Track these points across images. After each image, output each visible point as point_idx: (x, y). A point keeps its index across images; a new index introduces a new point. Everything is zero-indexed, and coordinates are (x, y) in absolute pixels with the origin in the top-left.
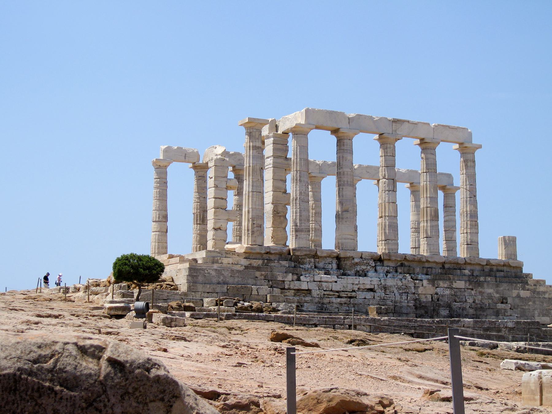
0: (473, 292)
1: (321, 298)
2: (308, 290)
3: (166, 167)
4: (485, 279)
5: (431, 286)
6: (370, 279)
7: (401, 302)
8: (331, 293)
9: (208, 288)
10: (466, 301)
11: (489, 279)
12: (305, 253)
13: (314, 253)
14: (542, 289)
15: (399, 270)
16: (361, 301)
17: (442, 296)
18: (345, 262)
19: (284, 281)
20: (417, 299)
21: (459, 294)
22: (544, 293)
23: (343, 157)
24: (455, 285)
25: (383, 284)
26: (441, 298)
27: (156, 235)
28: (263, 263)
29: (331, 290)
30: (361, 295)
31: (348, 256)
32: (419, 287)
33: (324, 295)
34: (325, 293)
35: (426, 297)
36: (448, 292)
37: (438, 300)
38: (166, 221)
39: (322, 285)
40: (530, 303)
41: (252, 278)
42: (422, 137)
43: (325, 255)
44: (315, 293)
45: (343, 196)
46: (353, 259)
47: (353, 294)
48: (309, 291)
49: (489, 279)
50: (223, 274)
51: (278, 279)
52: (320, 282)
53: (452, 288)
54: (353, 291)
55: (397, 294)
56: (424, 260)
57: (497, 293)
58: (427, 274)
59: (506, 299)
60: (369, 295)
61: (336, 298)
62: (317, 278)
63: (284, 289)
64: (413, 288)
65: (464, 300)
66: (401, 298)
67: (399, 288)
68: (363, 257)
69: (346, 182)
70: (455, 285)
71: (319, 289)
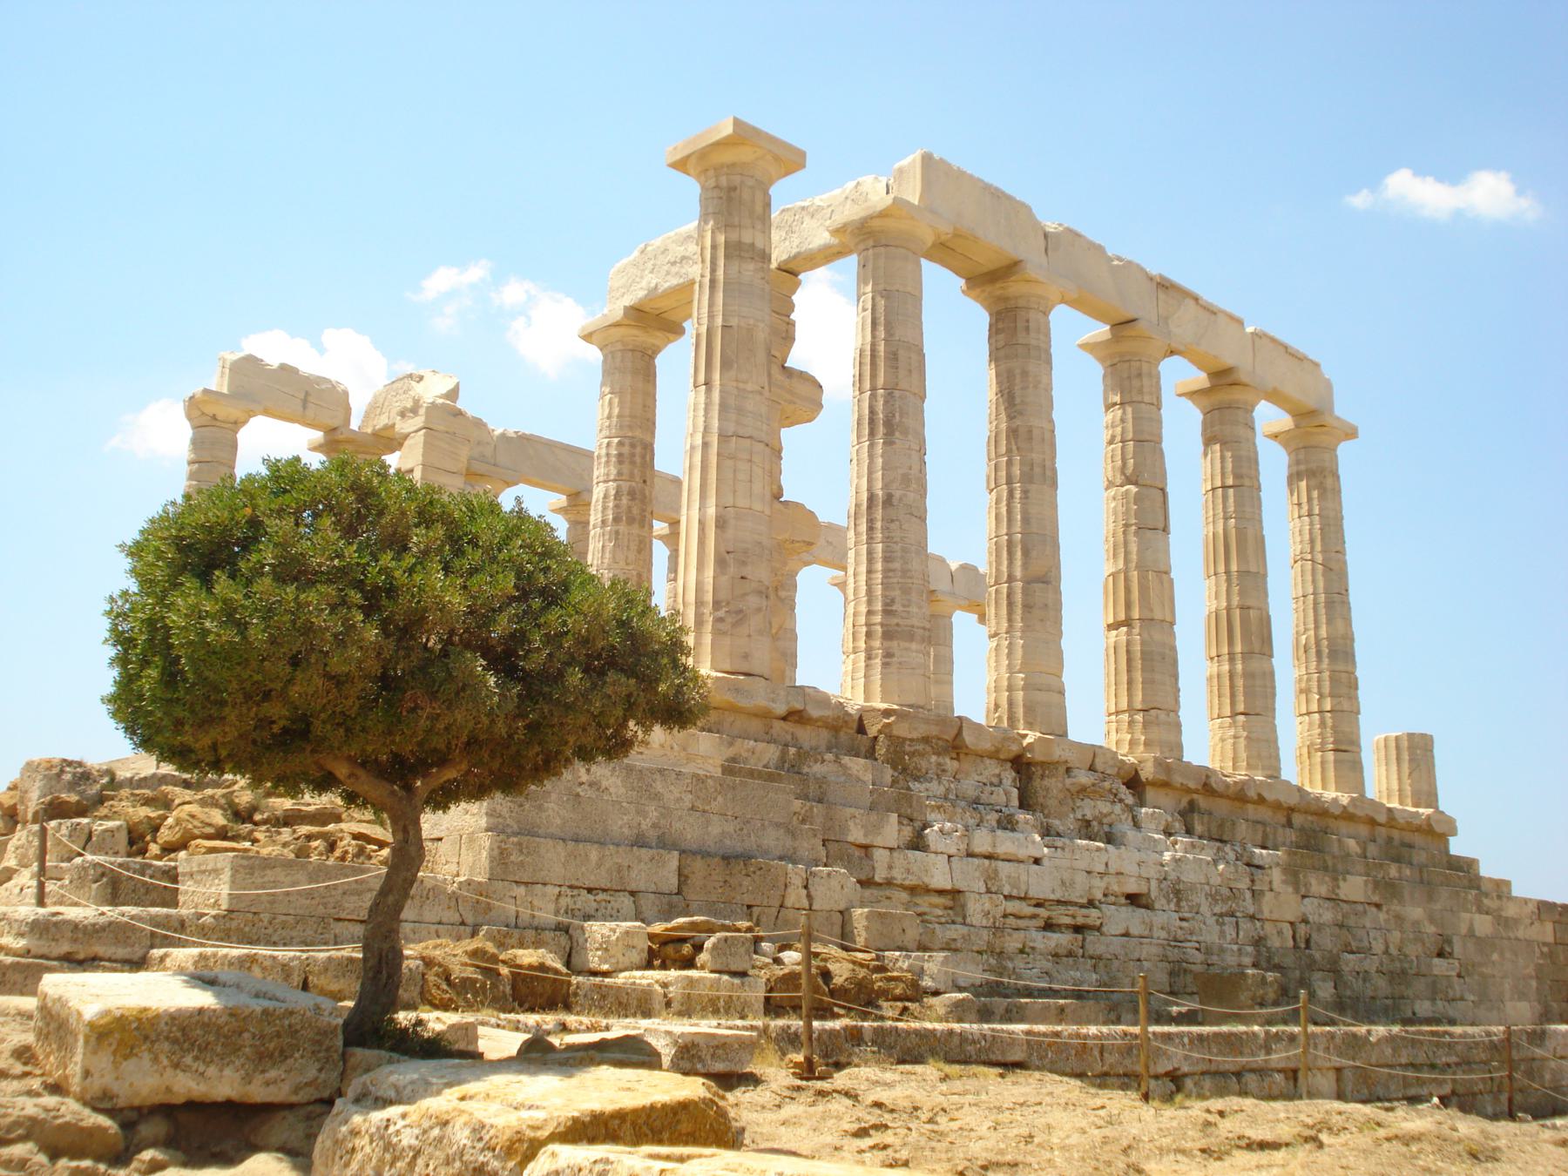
0: (1382, 916)
1: (997, 929)
2: (955, 893)
3: (237, 424)
5: (1290, 889)
6: (1137, 856)
7: (1222, 950)
9: (595, 865)
12: (921, 730)
13: (954, 732)
14: (1511, 911)
15: (1198, 828)
16: (1116, 945)
17: (1320, 928)
18: (1046, 782)
19: (866, 847)
21: (1351, 922)
22: (1516, 921)
23: (1025, 374)
25: (1172, 876)
26: (1315, 936)
28: (783, 758)
31: (1055, 758)
32: (1262, 892)
34: (1012, 907)
35: (1280, 933)
36: (1328, 916)
37: (1308, 942)
39: (996, 871)
40: (1495, 957)
41: (778, 825)
42: (1228, 360)
43: (987, 746)
44: (977, 908)
46: (1068, 770)
47: (1094, 913)
50: (657, 797)
51: (850, 839)
52: (989, 857)
53: (1333, 900)
54: (1091, 904)
55: (1211, 921)
56: (1252, 794)
57: (1432, 920)
58: (1264, 847)
59: (1449, 942)
60: (1132, 919)
62: (982, 841)
64: (1248, 895)
66: (1222, 933)
68: (1099, 766)
69: (1037, 470)
71: (989, 891)
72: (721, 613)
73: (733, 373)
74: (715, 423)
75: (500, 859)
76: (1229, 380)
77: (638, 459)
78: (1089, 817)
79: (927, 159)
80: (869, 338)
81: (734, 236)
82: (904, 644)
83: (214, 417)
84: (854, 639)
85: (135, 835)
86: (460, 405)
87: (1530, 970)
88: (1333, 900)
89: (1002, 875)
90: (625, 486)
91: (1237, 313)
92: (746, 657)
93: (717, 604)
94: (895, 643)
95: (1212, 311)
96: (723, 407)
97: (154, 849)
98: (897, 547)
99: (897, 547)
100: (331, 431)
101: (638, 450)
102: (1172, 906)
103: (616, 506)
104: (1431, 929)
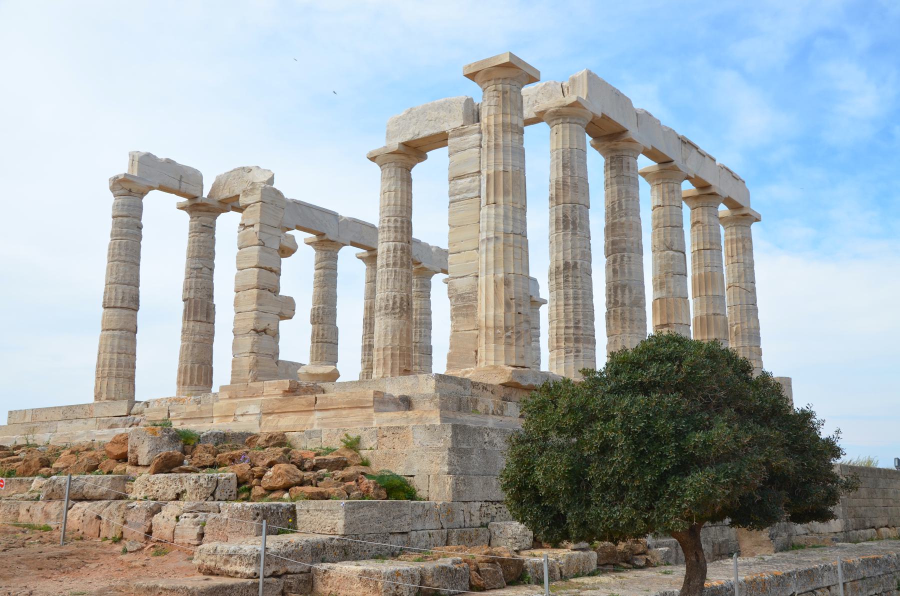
3: (143, 194)
23: (627, 192)
27: (113, 336)
38: (136, 310)
42: (710, 181)
45: (630, 273)
72: (509, 334)
73: (511, 198)
74: (502, 226)
75: (457, 492)
76: (709, 192)
77: (405, 230)
79: (589, 73)
80: (561, 175)
81: (508, 119)
82: (586, 345)
83: (130, 191)
84: (557, 342)
85: (240, 480)
86: (274, 186)
90: (399, 245)
91: (713, 156)
92: (523, 357)
93: (507, 329)
94: (581, 345)
96: (506, 217)
97: (258, 491)
98: (580, 291)
99: (580, 291)
100: (193, 198)
101: (405, 225)
103: (395, 256)
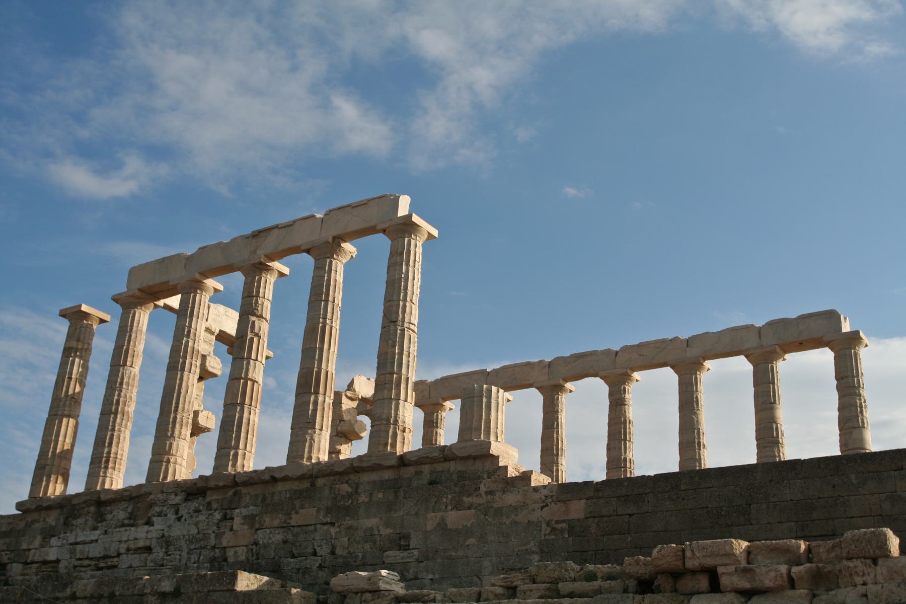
0: (333, 531)
4: (371, 495)
5: (246, 527)
8: (86, 562)
10: (315, 554)
11: (380, 495)
15: (214, 506)
17: (265, 546)
20: (215, 558)
22: (516, 509)
24: (295, 520)
26: (262, 551)
29: (88, 558)
30: (126, 561)
32: (224, 533)
33: (75, 567)
36: (278, 537)
40: (471, 541)
48: (58, 561)
49: (380, 495)
52: (77, 543)
56: (267, 477)
57: (387, 525)
59: (407, 537)
61: (92, 570)
63: (26, 563)
64: (213, 536)
65: (310, 550)
66: (189, 559)
67: (191, 540)
70: (295, 520)
78: (150, 515)
87: (532, 546)
88: (286, 527)
89: (78, 551)
95: (289, 226)
102: (164, 550)
104: (389, 531)
